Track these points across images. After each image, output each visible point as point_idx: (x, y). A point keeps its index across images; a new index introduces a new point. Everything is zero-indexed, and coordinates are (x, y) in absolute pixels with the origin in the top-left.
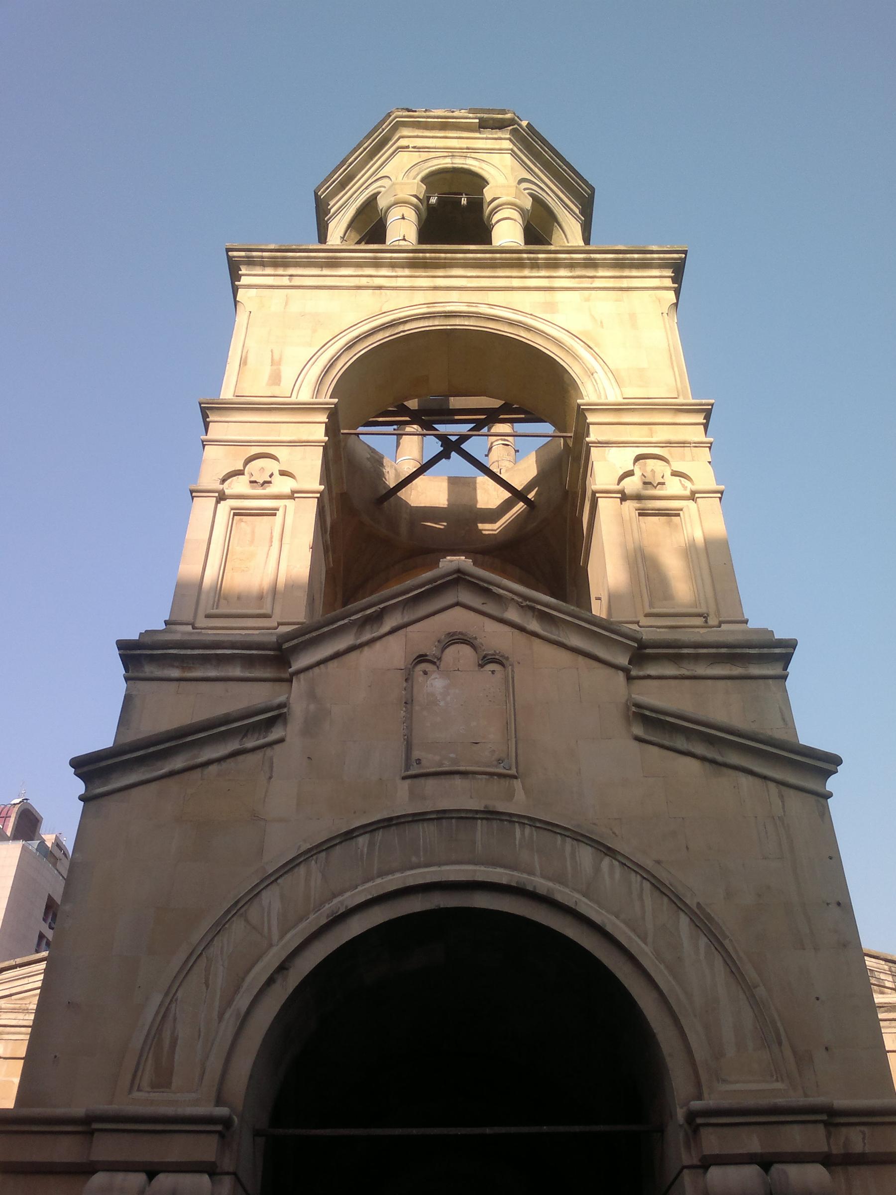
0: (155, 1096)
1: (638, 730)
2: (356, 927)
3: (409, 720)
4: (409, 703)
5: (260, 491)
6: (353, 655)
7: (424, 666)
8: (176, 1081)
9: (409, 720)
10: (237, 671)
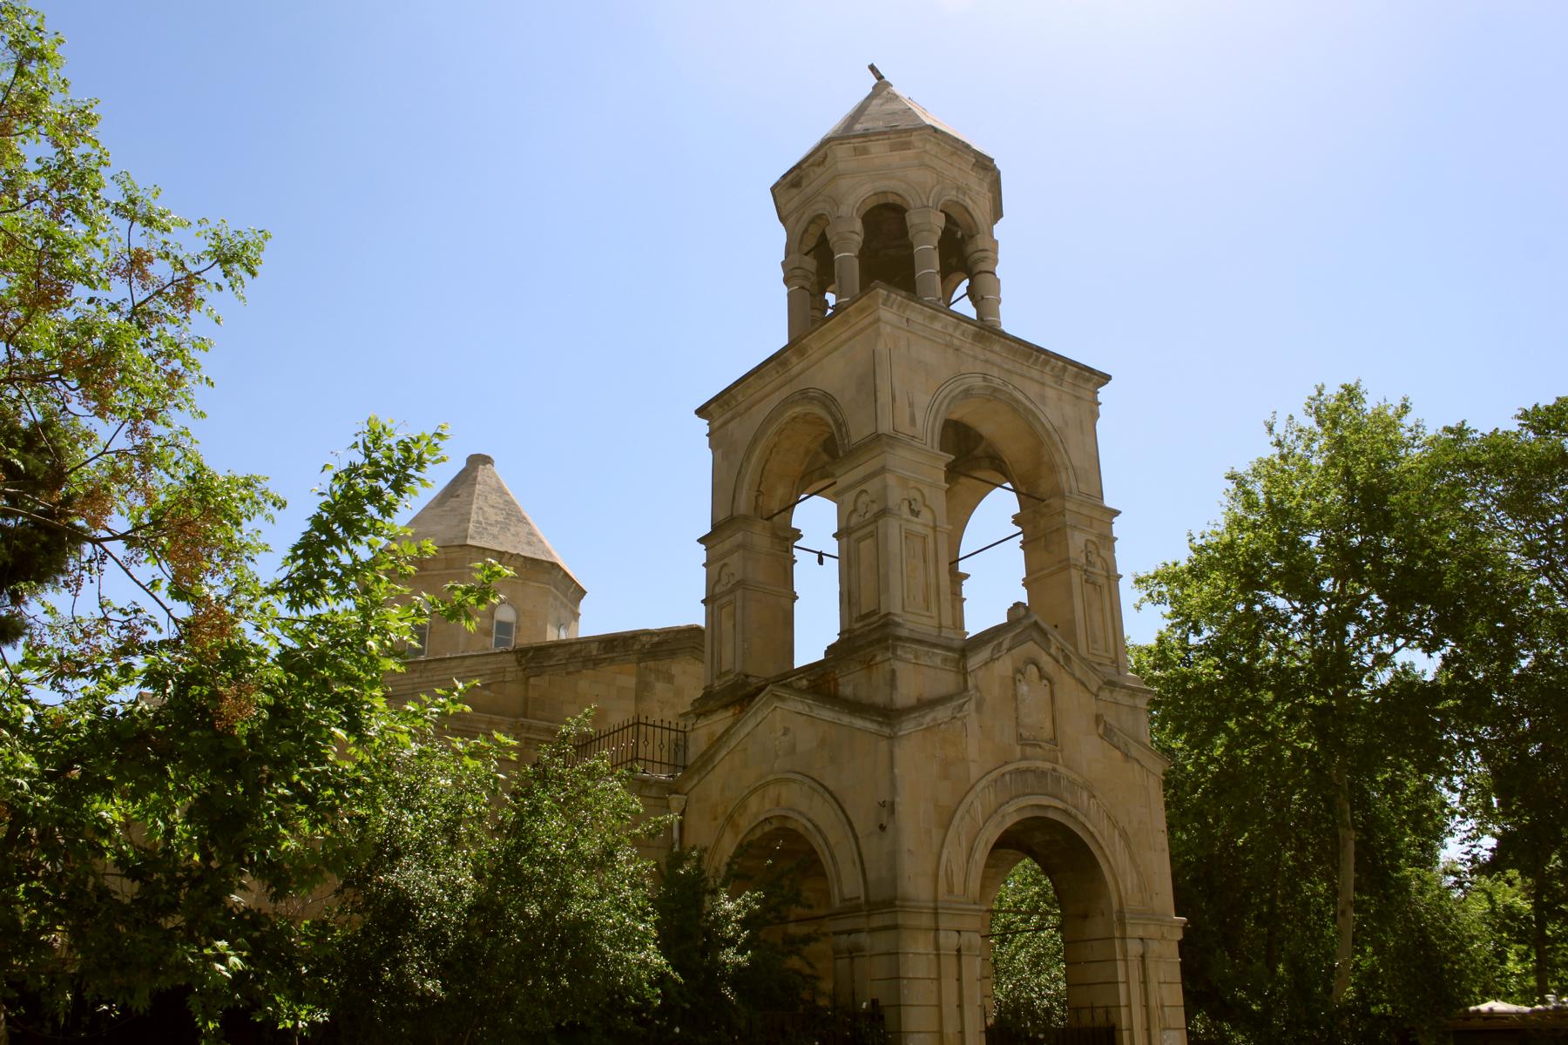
3: (1016, 709)
4: (1015, 697)
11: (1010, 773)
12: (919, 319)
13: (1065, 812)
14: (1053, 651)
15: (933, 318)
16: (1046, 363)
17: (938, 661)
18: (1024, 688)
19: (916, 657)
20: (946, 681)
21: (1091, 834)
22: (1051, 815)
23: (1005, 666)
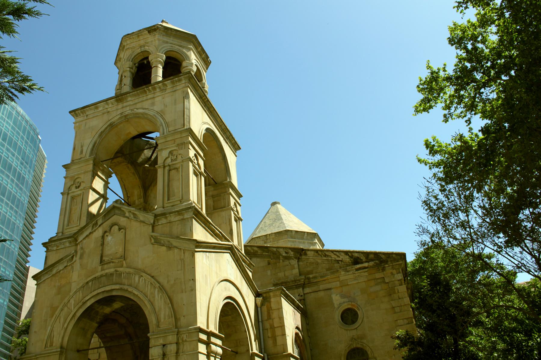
0: (50, 348)
2: (89, 304)
4: (103, 244)
6: (91, 235)
7: (107, 234)
8: (54, 344)
9: (102, 250)
11: (92, 280)
12: (92, 111)
13: (121, 289)
14: (127, 214)
15: (97, 108)
16: (154, 89)
17: (67, 244)
18: (109, 239)
19: (58, 247)
20: (72, 250)
21: (137, 296)
22: (114, 293)
23: (99, 232)
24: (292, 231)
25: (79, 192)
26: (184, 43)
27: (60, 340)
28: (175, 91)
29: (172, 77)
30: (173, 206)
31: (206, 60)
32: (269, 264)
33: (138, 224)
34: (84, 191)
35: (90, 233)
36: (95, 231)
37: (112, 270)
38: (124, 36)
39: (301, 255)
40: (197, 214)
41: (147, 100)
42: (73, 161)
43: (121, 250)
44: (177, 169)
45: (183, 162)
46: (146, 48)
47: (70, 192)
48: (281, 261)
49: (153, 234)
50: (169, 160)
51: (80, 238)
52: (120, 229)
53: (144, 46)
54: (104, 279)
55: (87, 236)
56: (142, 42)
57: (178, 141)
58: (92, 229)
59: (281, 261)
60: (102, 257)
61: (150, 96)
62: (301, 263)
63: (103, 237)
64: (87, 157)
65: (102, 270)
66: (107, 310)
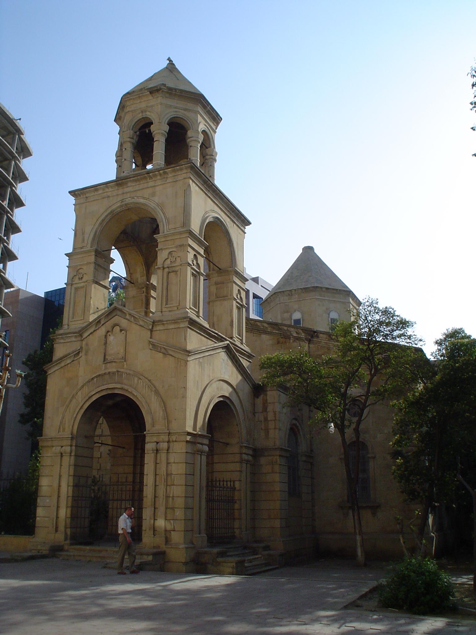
1: (151, 346)
2: (94, 398)
4: (106, 343)
5: (81, 281)
9: (105, 349)
10: (74, 339)
18: (111, 338)
21: (135, 396)
22: (116, 392)
23: (102, 331)
24: (321, 288)
25: (82, 284)
26: (190, 106)
27: (71, 427)
28: (176, 181)
29: (173, 166)
30: (170, 311)
31: (216, 118)
32: (278, 343)
33: (138, 327)
34: (86, 283)
35: (94, 331)
36: (98, 329)
37: (115, 370)
38: (124, 95)
39: (312, 337)
40: (193, 323)
41: (147, 188)
42: (74, 249)
43: (122, 351)
44: (176, 272)
45: (181, 265)
46: (148, 113)
47: (74, 283)
48: (291, 341)
49: (151, 340)
50: (168, 262)
51: (85, 335)
52: (121, 330)
53: (146, 112)
54: (107, 377)
55: (91, 333)
56: (143, 105)
57: (178, 243)
58: (96, 327)
59: (291, 341)
60: (105, 356)
61: (151, 184)
62: (311, 346)
63: (106, 336)
64: (89, 248)
65: (106, 369)
66: (110, 402)
